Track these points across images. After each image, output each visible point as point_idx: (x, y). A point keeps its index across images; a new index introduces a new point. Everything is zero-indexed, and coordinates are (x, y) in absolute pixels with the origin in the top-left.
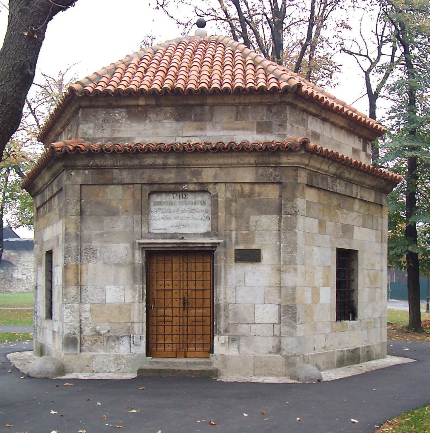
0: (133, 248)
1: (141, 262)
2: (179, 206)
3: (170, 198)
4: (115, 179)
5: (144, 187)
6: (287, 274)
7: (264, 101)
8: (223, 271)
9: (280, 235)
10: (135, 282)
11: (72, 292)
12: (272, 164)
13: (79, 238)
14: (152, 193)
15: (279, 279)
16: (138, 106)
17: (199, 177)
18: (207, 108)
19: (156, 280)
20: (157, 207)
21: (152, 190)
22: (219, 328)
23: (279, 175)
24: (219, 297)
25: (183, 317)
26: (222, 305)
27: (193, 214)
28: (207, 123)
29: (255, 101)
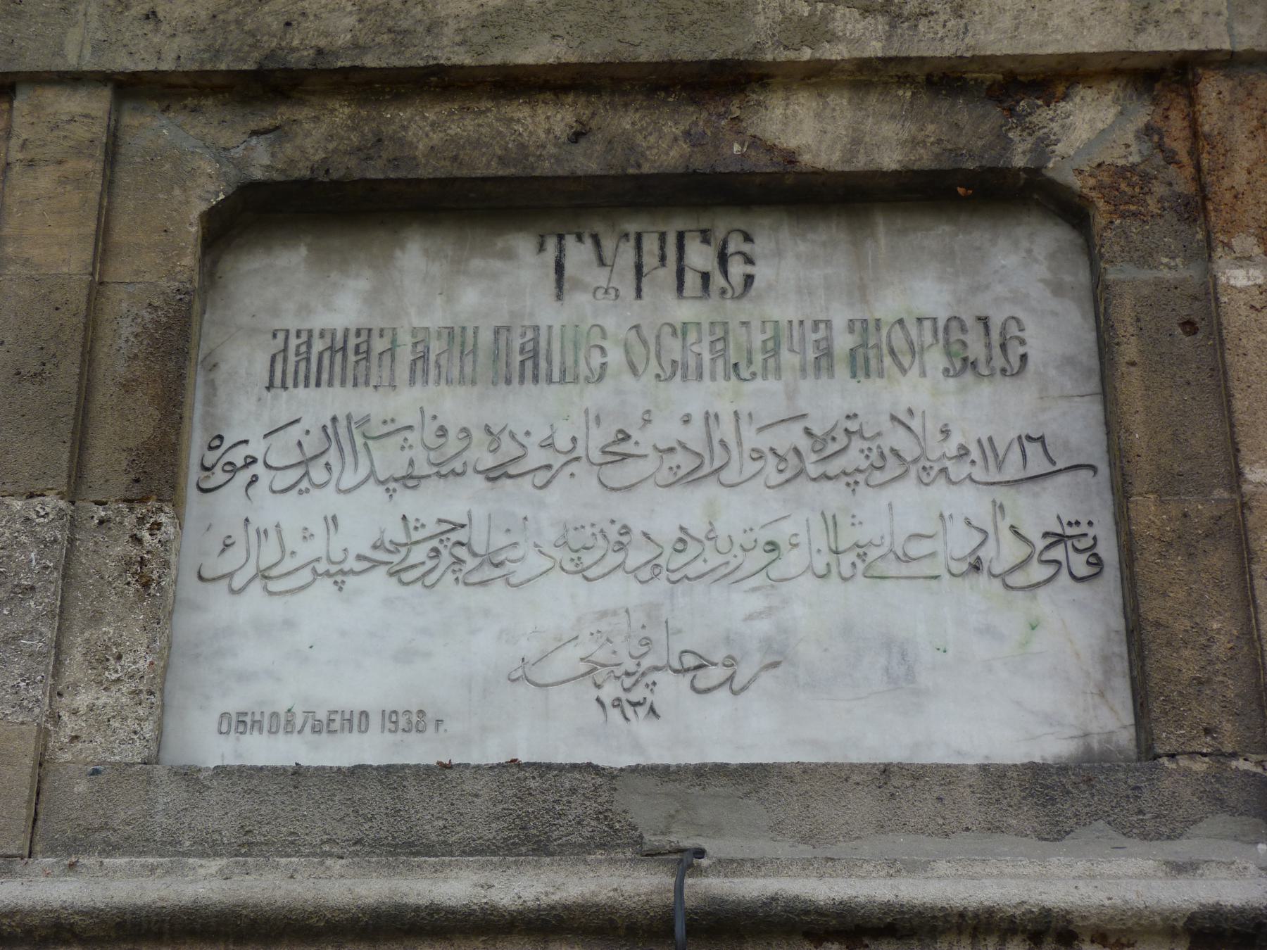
3: (505, 284)
5: (152, 129)
14: (252, 215)
20: (317, 405)
21: (261, 160)
27: (833, 495)
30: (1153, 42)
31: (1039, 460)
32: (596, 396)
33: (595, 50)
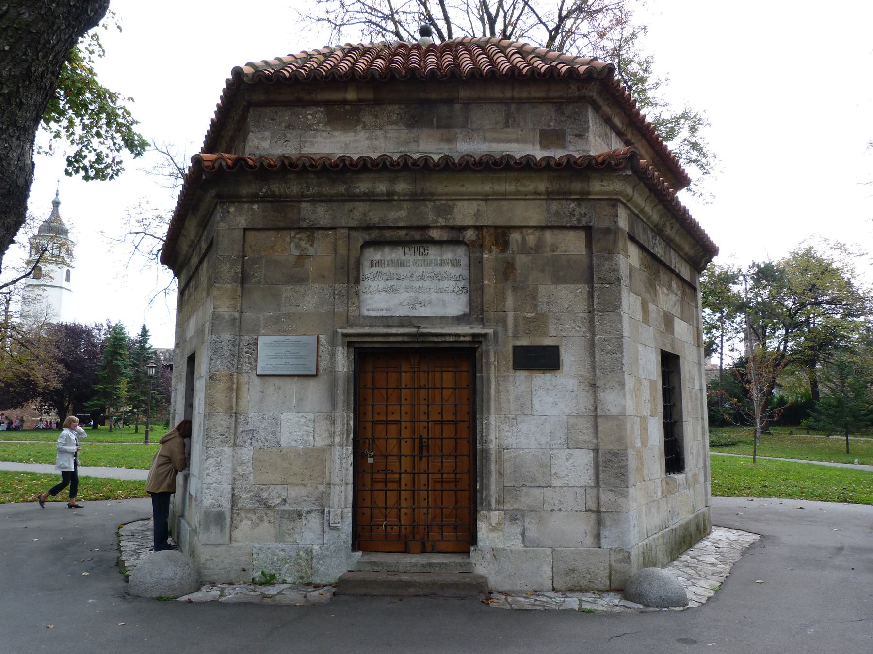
0: (333, 344)
1: (345, 369)
2: (414, 268)
3: (398, 254)
4: (304, 220)
5: (354, 234)
6: (607, 391)
7: (552, 94)
8: (493, 387)
9: (591, 321)
10: (334, 406)
11: (221, 426)
12: (576, 194)
13: (237, 324)
14: (366, 245)
15: (592, 401)
16: (344, 102)
17: (448, 216)
18: (457, 107)
19: (370, 403)
20: (376, 270)
21: (367, 238)
22: (486, 496)
23: (585, 214)
24: (488, 435)
25: (419, 473)
26: (492, 452)
28: (458, 131)
29: (538, 95)
30: (478, 224)
31: (461, 278)
32: (409, 269)
33: (409, 224)
